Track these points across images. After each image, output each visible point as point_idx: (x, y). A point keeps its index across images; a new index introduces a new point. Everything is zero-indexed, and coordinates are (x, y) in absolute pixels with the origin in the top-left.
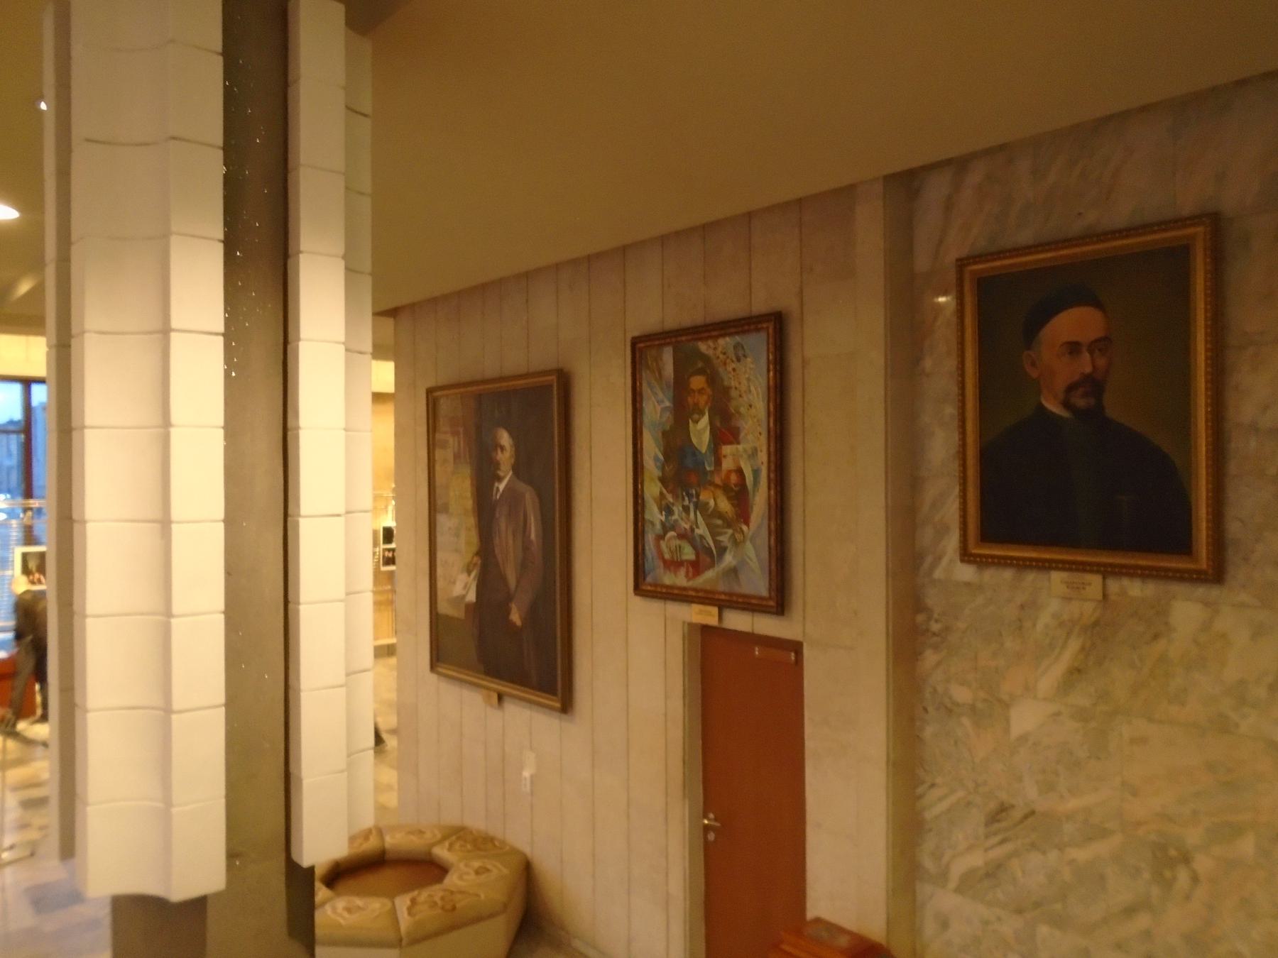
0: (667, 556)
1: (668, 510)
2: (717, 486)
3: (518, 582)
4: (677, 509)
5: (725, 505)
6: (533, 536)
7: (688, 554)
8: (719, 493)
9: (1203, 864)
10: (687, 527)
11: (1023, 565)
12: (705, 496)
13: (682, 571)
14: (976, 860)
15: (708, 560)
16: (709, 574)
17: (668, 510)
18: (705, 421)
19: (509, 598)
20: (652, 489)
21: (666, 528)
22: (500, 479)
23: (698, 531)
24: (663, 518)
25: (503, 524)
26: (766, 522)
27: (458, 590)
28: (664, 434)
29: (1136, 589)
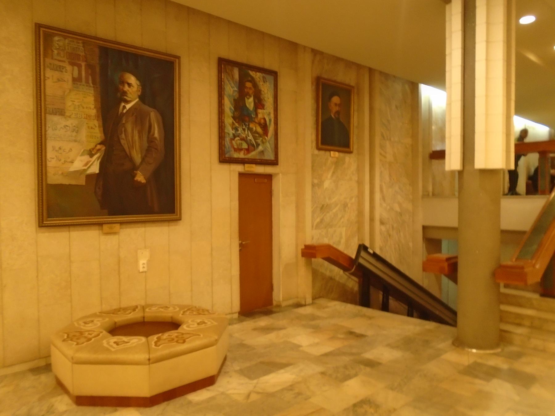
0: (236, 147)
1: (236, 129)
2: (256, 123)
3: (143, 159)
4: (240, 130)
5: (259, 130)
6: (156, 135)
7: (245, 146)
8: (257, 125)
9: (349, 205)
10: (244, 136)
11: (326, 150)
12: (251, 125)
13: (242, 152)
14: (318, 220)
15: (253, 148)
16: (253, 153)
17: (236, 129)
18: (251, 99)
19: (135, 168)
20: (228, 120)
21: (235, 136)
22: (127, 102)
23: (248, 138)
24: (234, 132)
25: (129, 127)
26: (273, 137)
27: (78, 164)
28: (234, 100)
29: (342, 155)
